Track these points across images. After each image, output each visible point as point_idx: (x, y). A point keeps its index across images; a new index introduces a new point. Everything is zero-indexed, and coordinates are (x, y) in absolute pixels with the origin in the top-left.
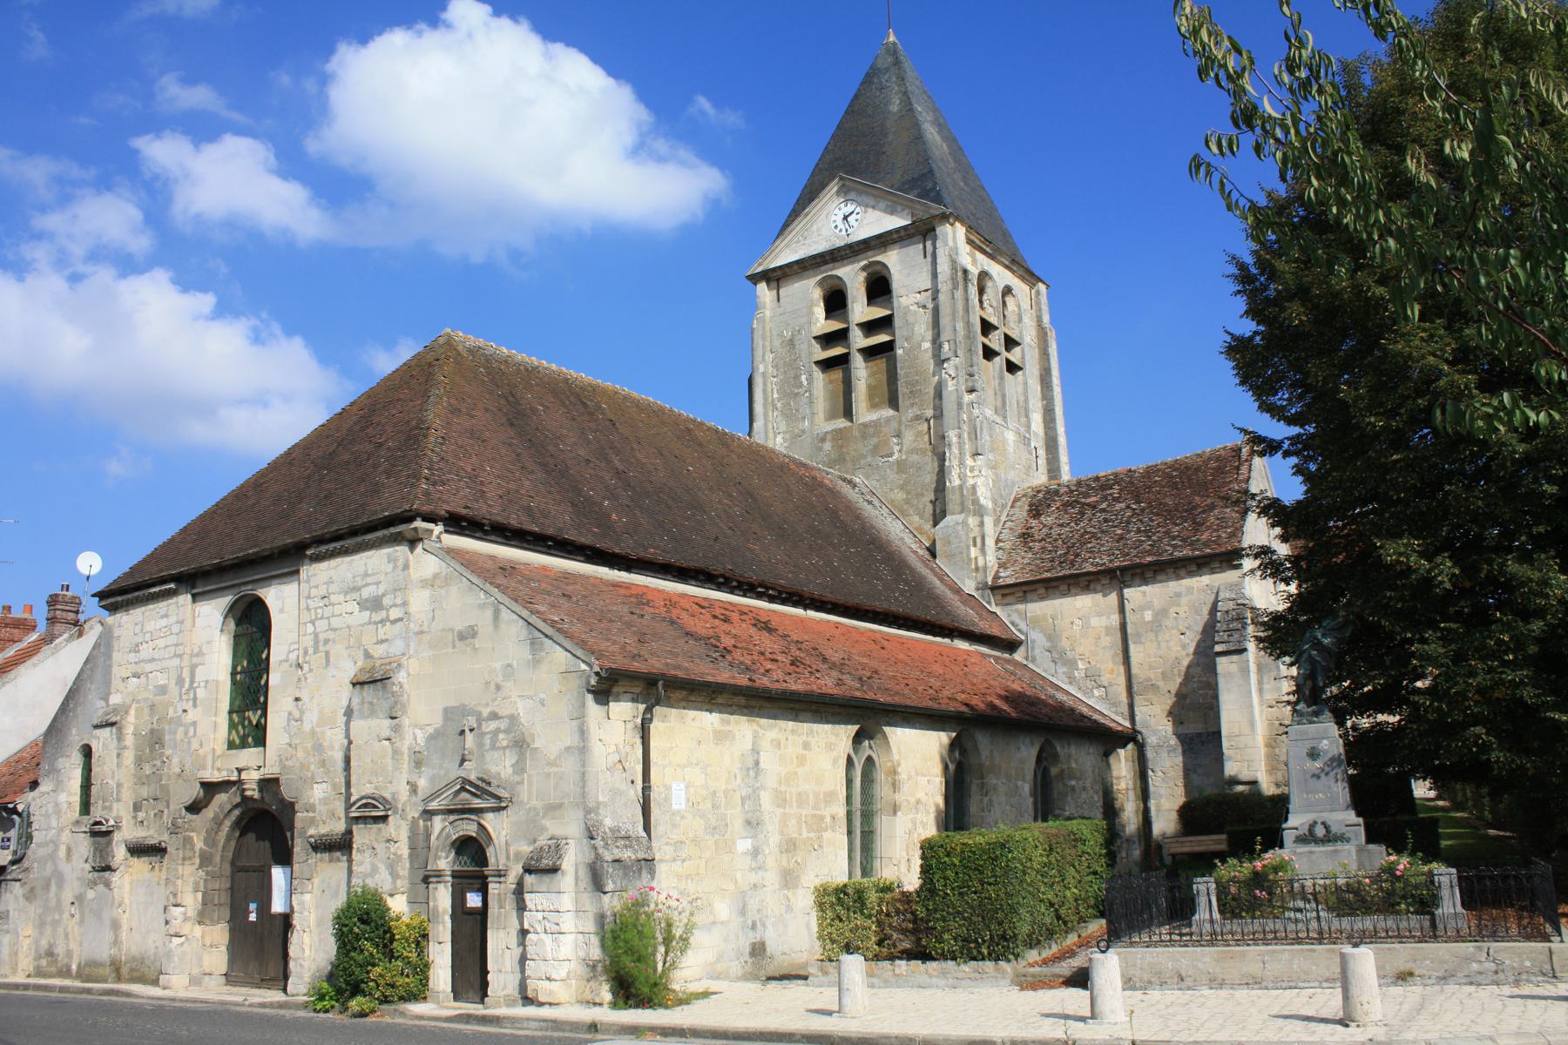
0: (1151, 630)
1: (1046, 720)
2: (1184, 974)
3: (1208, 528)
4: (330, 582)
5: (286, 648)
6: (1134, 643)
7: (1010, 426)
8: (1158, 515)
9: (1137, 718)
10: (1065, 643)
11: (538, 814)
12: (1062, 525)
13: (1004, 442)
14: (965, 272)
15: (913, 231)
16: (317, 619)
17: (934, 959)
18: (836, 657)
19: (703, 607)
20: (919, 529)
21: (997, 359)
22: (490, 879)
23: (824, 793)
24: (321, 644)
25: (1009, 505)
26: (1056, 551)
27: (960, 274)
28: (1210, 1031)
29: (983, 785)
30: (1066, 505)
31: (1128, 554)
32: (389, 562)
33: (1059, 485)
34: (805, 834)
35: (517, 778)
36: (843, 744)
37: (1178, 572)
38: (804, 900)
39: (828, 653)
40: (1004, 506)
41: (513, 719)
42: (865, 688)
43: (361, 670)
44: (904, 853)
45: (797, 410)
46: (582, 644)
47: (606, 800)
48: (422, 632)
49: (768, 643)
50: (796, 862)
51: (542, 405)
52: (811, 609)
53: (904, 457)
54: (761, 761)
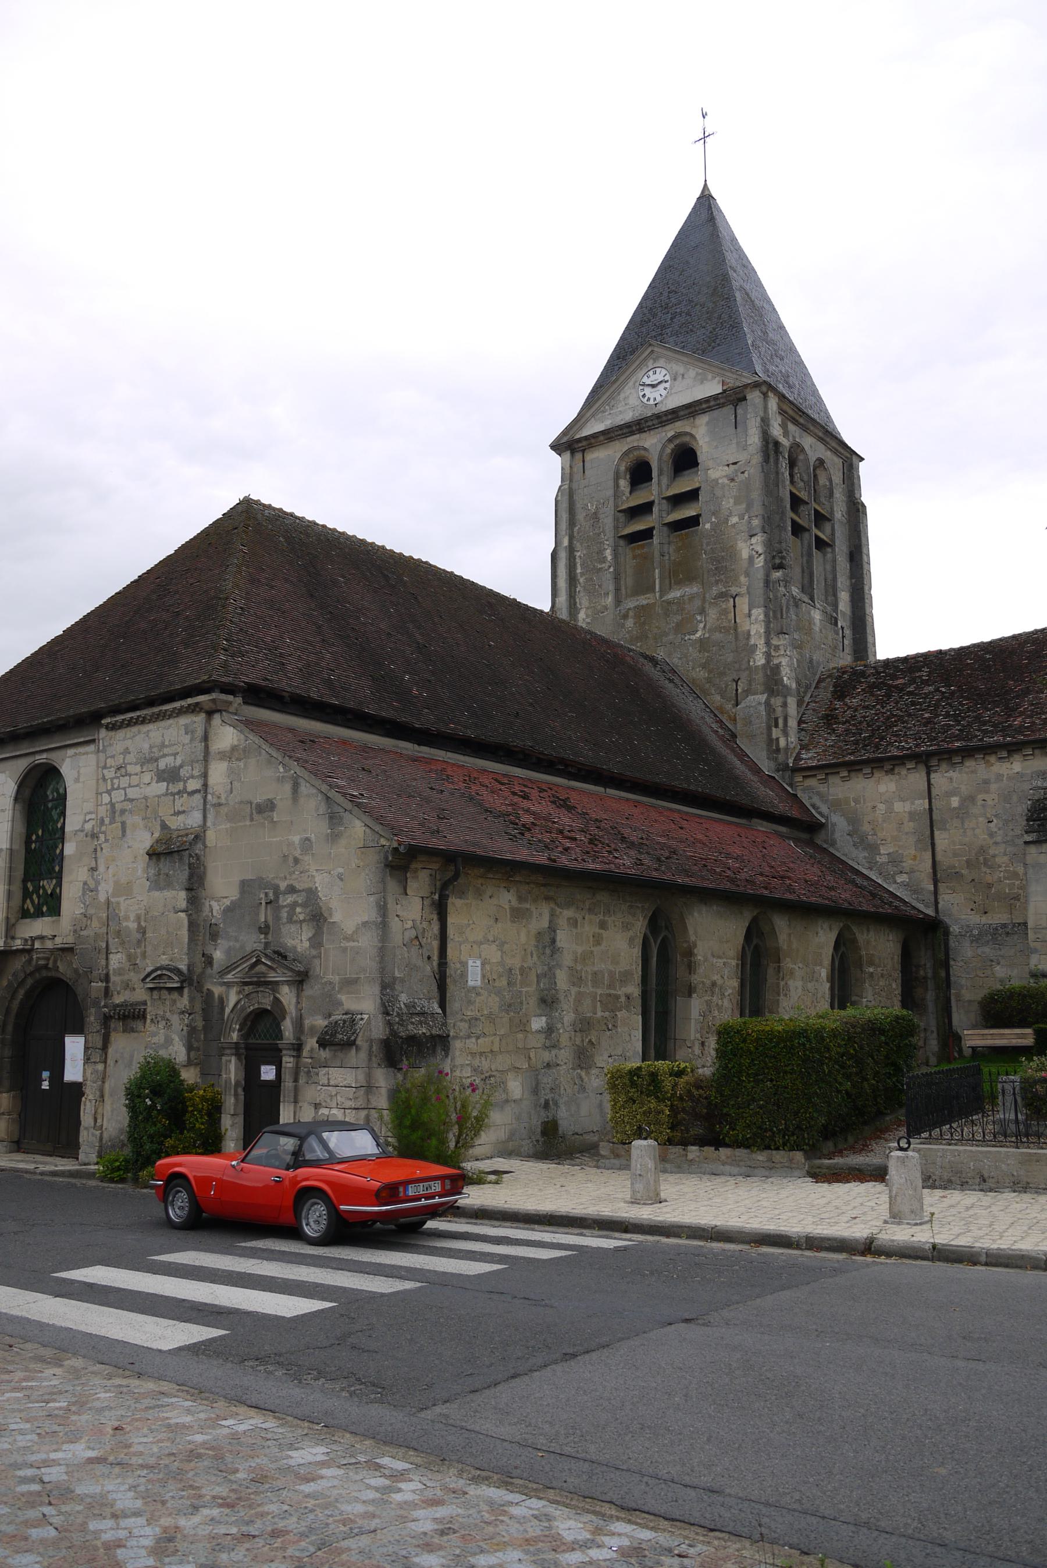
0: (958, 817)
1: (846, 905)
2: (986, 1175)
3: (1021, 714)
4: (127, 751)
5: (81, 818)
6: (939, 829)
7: (818, 605)
8: (967, 698)
9: (940, 906)
10: (866, 828)
11: (334, 988)
12: (867, 707)
13: (811, 621)
14: (777, 444)
15: (722, 401)
16: (113, 789)
17: (727, 1146)
18: (634, 837)
19: (503, 784)
20: (721, 709)
21: (806, 535)
22: (284, 1052)
23: (620, 972)
24: (117, 814)
25: (814, 686)
26: (861, 734)
27: (771, 446)
28: (1014, 1239)
29: (779, 970)
30: (872, 686)
31: (935, 739)
32: (186, 733)
33: (865, 666)
34: (599, 1014)
35: (314, 952)
36: (640, 924)
37: (987, 758)
38: (596, 1081)
39: (626, 832)
40: (808, 687)
41: (312, 894)
42: (663, 868)
43: (157, 841)
44: (698, 1036)
45: (600, 586)
46: (379, 820)
47: (402, 975)
48: (220, 805)
49: (565, 819)
50: (590, 1041)
51: (343, 577)
52: (610, 787)
53: (707, 635)
54: (558, 938)
